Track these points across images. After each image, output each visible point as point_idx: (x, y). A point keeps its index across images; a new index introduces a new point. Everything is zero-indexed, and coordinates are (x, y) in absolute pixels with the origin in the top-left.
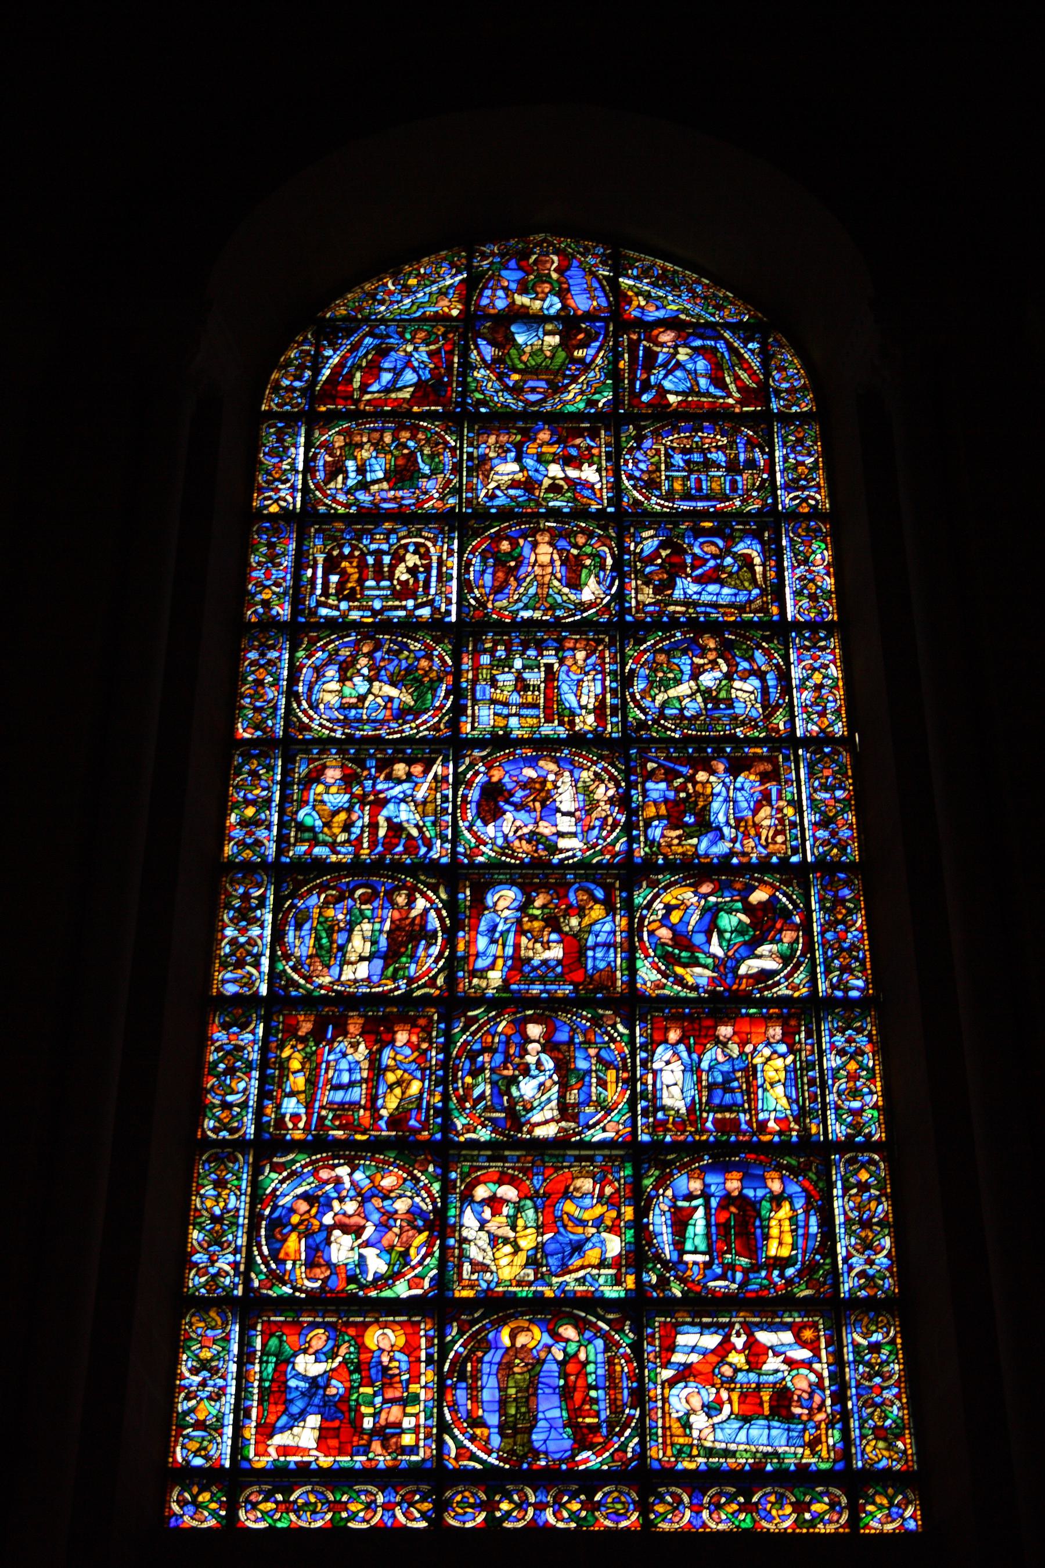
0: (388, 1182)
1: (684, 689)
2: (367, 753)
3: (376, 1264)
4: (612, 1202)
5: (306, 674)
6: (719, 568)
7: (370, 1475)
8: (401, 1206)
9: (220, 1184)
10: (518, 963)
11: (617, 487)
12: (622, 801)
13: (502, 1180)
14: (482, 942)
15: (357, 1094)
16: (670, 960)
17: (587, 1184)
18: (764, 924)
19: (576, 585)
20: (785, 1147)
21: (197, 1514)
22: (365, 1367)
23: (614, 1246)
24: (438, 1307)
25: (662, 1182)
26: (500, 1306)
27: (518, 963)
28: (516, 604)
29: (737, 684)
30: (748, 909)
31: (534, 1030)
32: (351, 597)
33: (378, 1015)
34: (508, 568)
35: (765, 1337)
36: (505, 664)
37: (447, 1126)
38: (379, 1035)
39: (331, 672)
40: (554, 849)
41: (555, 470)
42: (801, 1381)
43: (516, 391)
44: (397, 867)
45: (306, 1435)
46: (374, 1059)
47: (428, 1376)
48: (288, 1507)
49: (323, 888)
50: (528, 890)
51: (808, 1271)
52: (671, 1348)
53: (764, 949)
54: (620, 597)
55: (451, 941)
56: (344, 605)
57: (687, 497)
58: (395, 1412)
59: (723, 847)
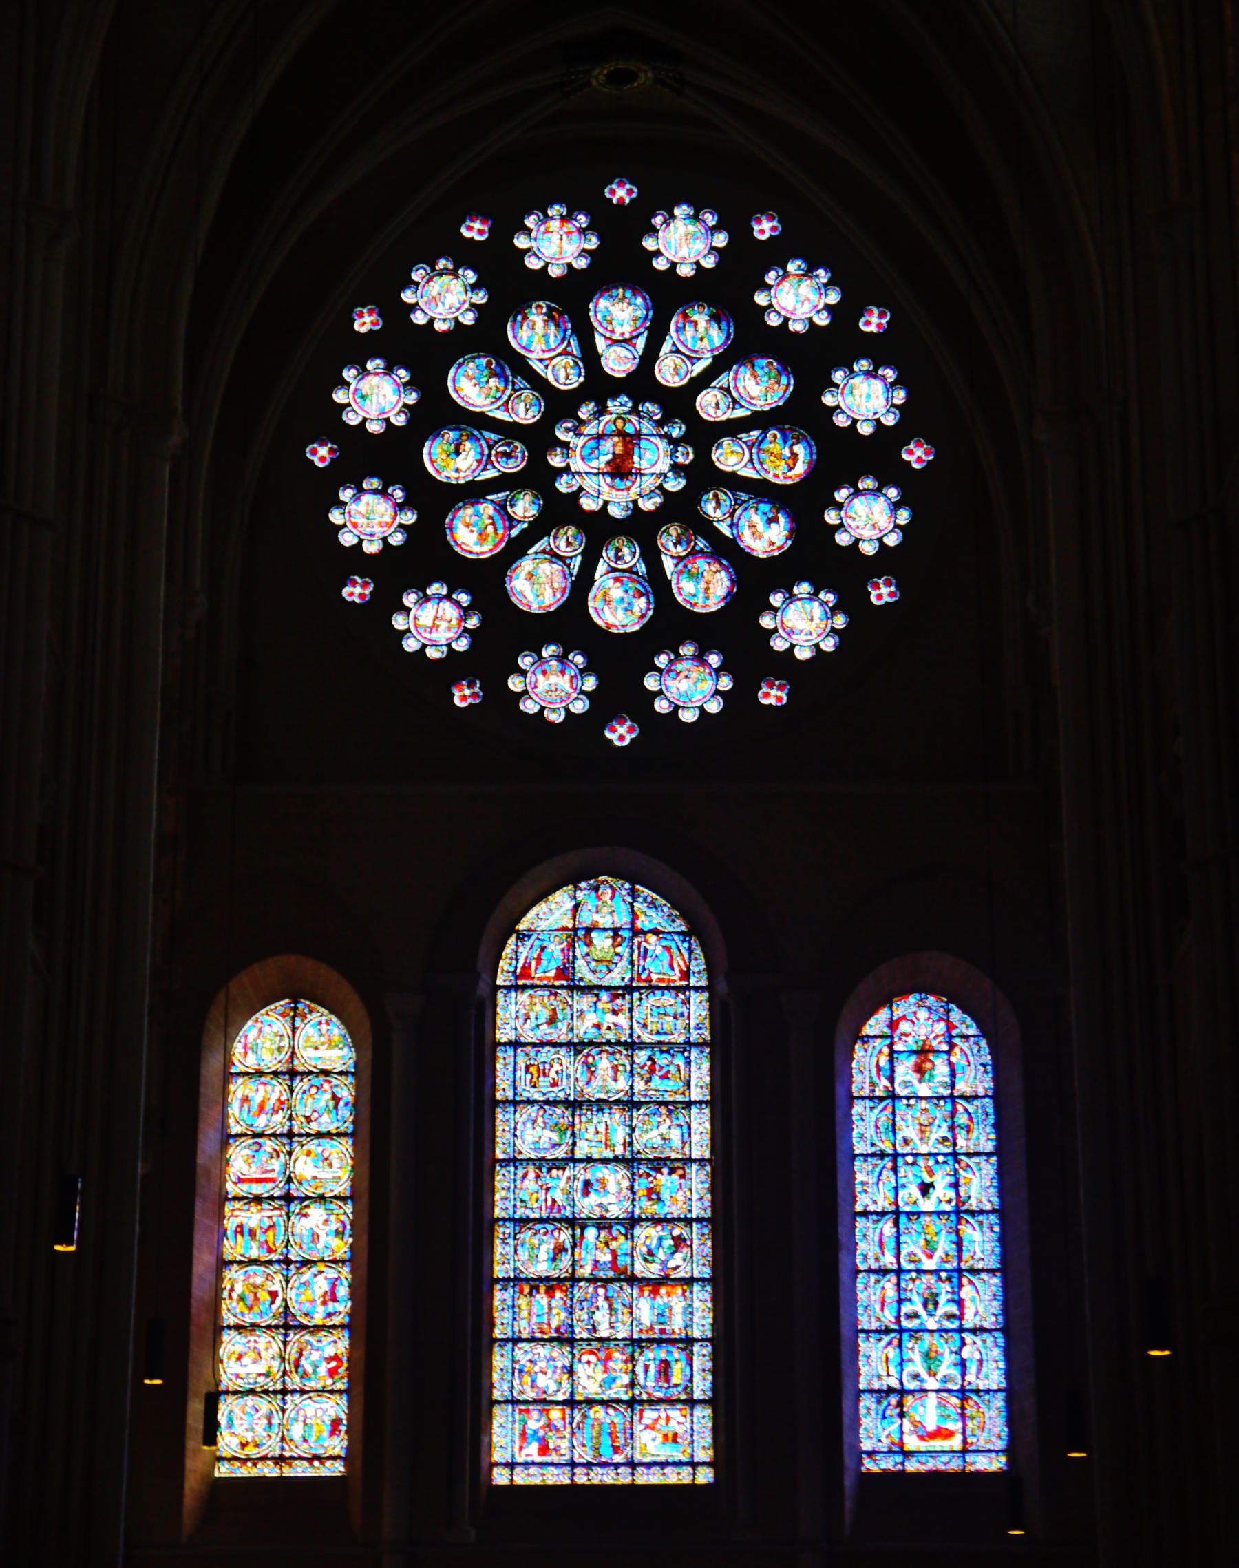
0: (555, 1354)
1: (655, 1133)
2: (545, 1165)
3: (552, 1387)
4: (626, 1362)
5: (519, 1126)
6: (668, 1072)
7: (552, 1464)
8: (559, 1364)
9: (502, 1355)
10: (596, 1262)
11: (631, 1028)
12: (631, 1188)
13: (591, 1352)
14: (583, 1253)
15: (545, 1319)
16: (646, 1260)
17: (617, 1355)
18: (679, 1242)
19: (615, 1080)
20: (680, 1340)
21: (500, 1477)
22: (550, 1425)
23: (626, 1379)
24: (571, 1403)
25: (641, 1354)
26: (590, 1402)
27: (596, 1262)
28: (594, 1092)
29: (672, 1131)
30: (673, 1238)
31: (601, 1291)
32: (534, 1086)
33: (551, 1285)
34: (591, 1069)
35: (670, 1413)
36: (590, 1120)
37: (573, 1332)
38: (550, 1293)
39: (529, 1125)
40: (607, 1211)
41: (610, 1019)
42: (680, 1430)
43: (594, 972)
44: (555, 1219)
45: (532, 1450)
46: (549, 1305)
47: (569, 1430)
48: (528, 1475)
49: (530, 1229)
50: (599, 1228)
51: (685, 1388)
52: (641, 1417)
53: (678, 1256)
54: (632, 1087)
55: (573, 1254)
56: (533, 1090)
57: (658, 1033)
58: (559, 1442)
59: (666, 1209)
